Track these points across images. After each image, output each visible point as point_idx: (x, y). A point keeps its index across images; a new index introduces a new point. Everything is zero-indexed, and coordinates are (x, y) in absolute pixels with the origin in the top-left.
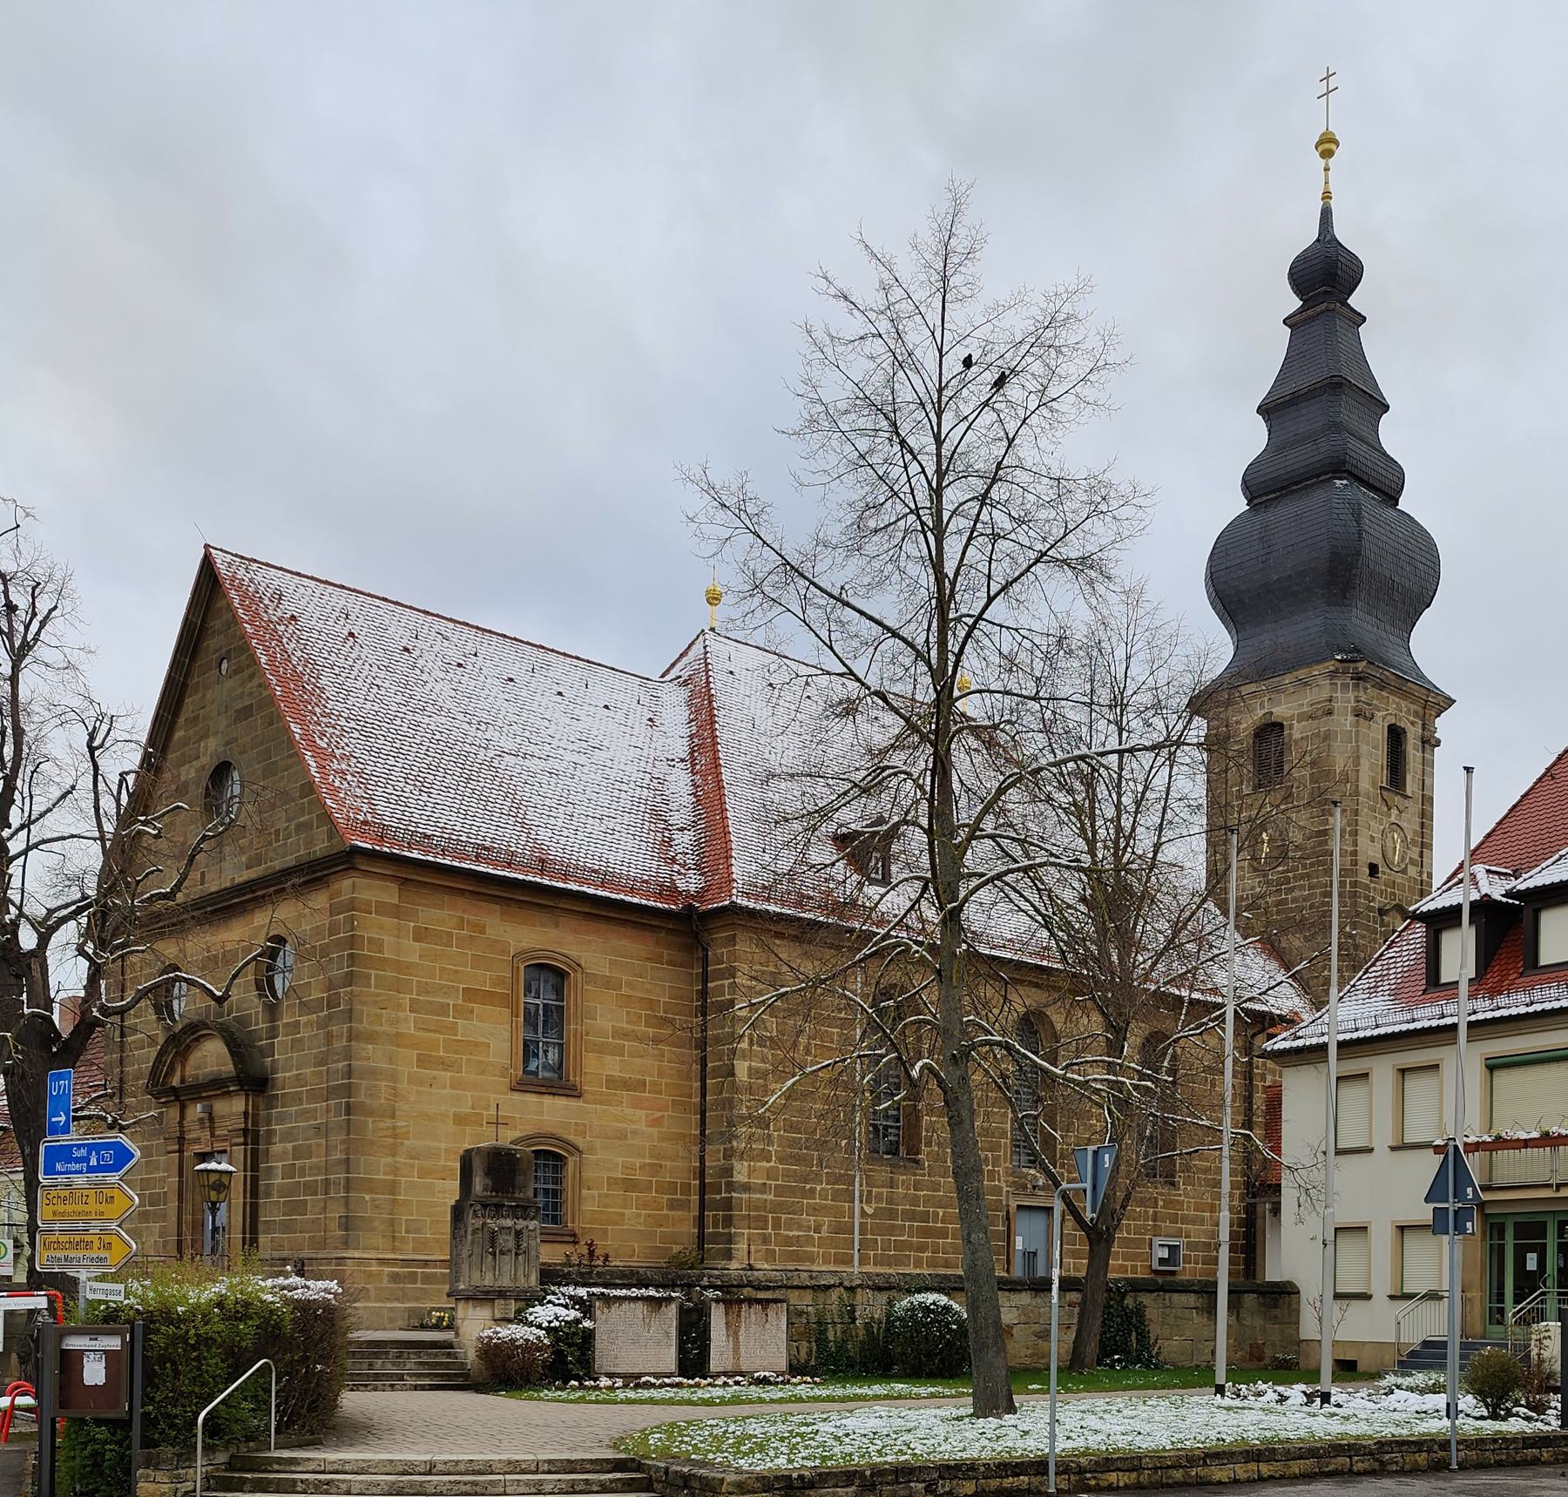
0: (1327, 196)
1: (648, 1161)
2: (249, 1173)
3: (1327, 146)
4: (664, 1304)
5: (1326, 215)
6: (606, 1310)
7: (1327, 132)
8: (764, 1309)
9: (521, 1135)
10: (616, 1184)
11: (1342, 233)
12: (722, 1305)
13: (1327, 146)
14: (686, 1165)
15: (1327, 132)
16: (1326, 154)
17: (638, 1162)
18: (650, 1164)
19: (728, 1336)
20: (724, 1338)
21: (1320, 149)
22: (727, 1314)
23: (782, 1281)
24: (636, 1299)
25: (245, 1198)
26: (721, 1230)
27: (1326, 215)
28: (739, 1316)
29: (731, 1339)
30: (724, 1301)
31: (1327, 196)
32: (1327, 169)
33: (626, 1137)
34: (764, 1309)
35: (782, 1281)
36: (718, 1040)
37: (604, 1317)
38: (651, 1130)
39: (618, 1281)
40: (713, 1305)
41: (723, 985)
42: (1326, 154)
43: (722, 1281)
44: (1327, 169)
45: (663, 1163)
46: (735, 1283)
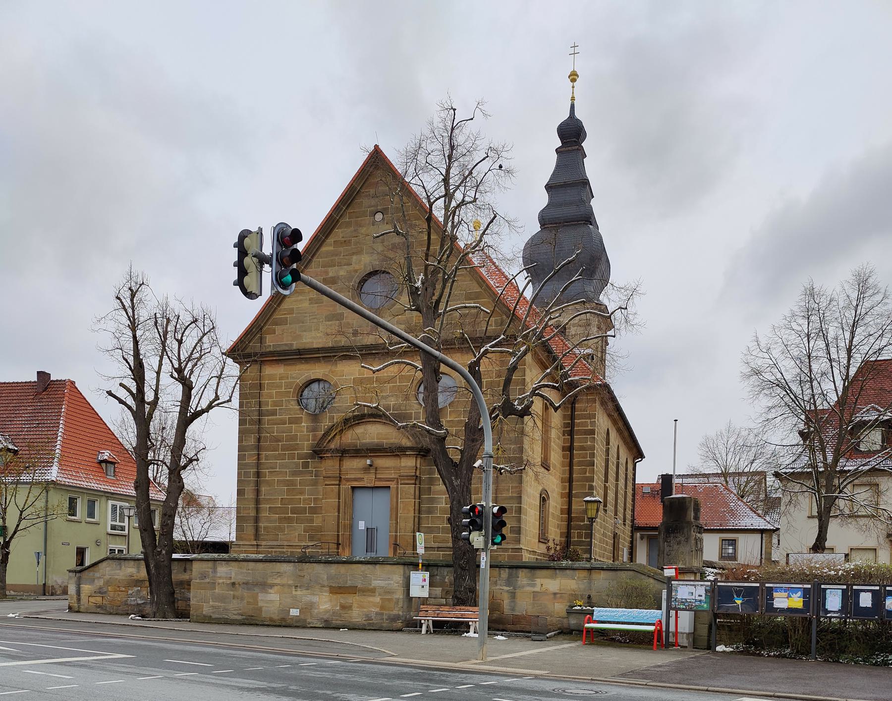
0: (573, 99)
2: (417, 501)
3: (573, 77)
5: (572, 107)
7: (574, 71)
11: (578, 115)
13: (573, 77)
15: (574, 71)
16: (573, 81)
21: (571, 78)
25: (415, 513)
26: (584, 539)
27: (572, 107)
31: (573, 99)
32: (573, 87)
36: (582, 448)
41: (271, 406)
42: (573, 81)
44: (573, 87)
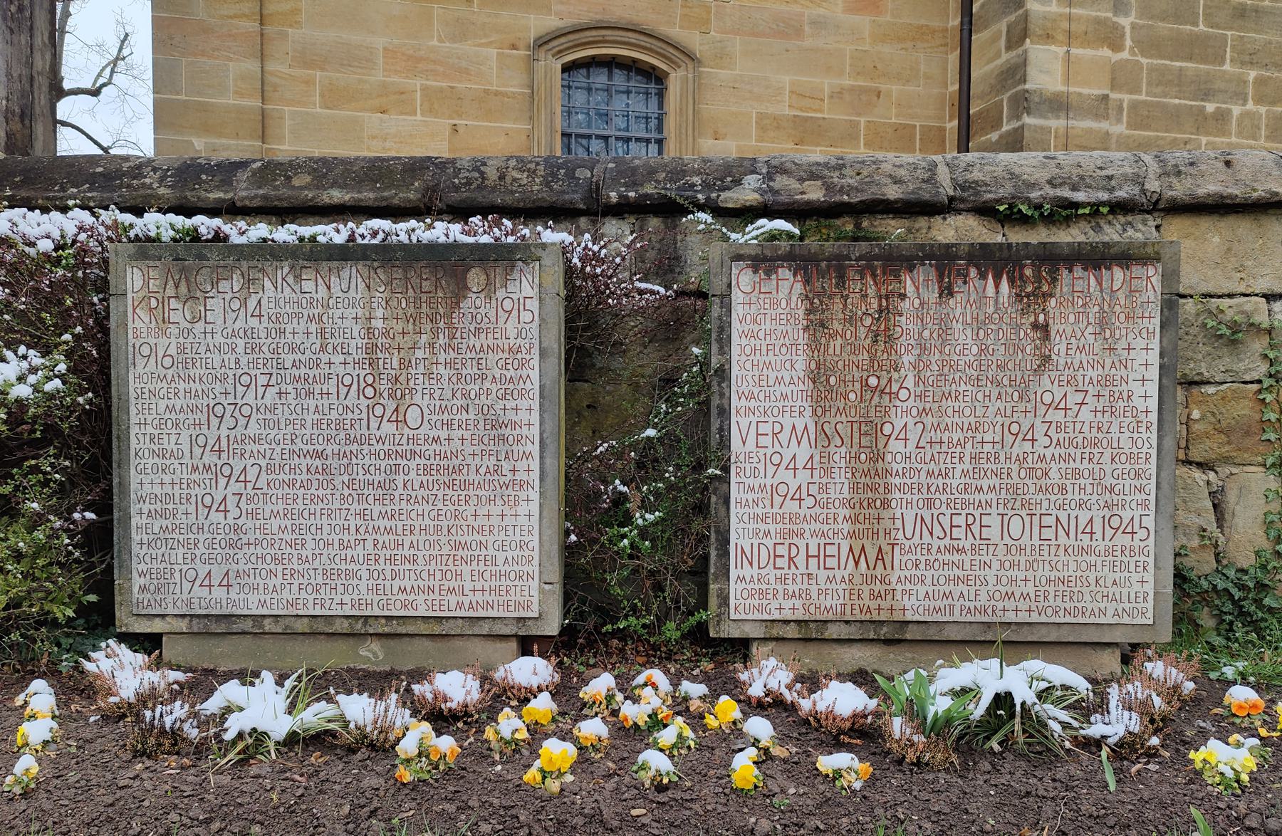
1: (847, 82)
4: (475, 278)
6: (179, 313)
8: (1031, 298)
9: (561, 24)
10: (778, 128)
12: (787, 285)
14: (936, 91)
17: (827, 84)
18: (852, 89)
19: (823, 436)
20: (804, 452)
22: (817, 325)
23: (1138, 180)
24: (347, 253)
28: (884, 335)
29: (839, 454)
30: (803, 263)
33: (799, 32)
34: (1031, 298)
35: (1138, 180)
37: (168, 344)
38: (856, 19)
39: (337, 196)
40: (744, 279)
43: (829, 188)
45: (883, 87)
46: (893, 193)
